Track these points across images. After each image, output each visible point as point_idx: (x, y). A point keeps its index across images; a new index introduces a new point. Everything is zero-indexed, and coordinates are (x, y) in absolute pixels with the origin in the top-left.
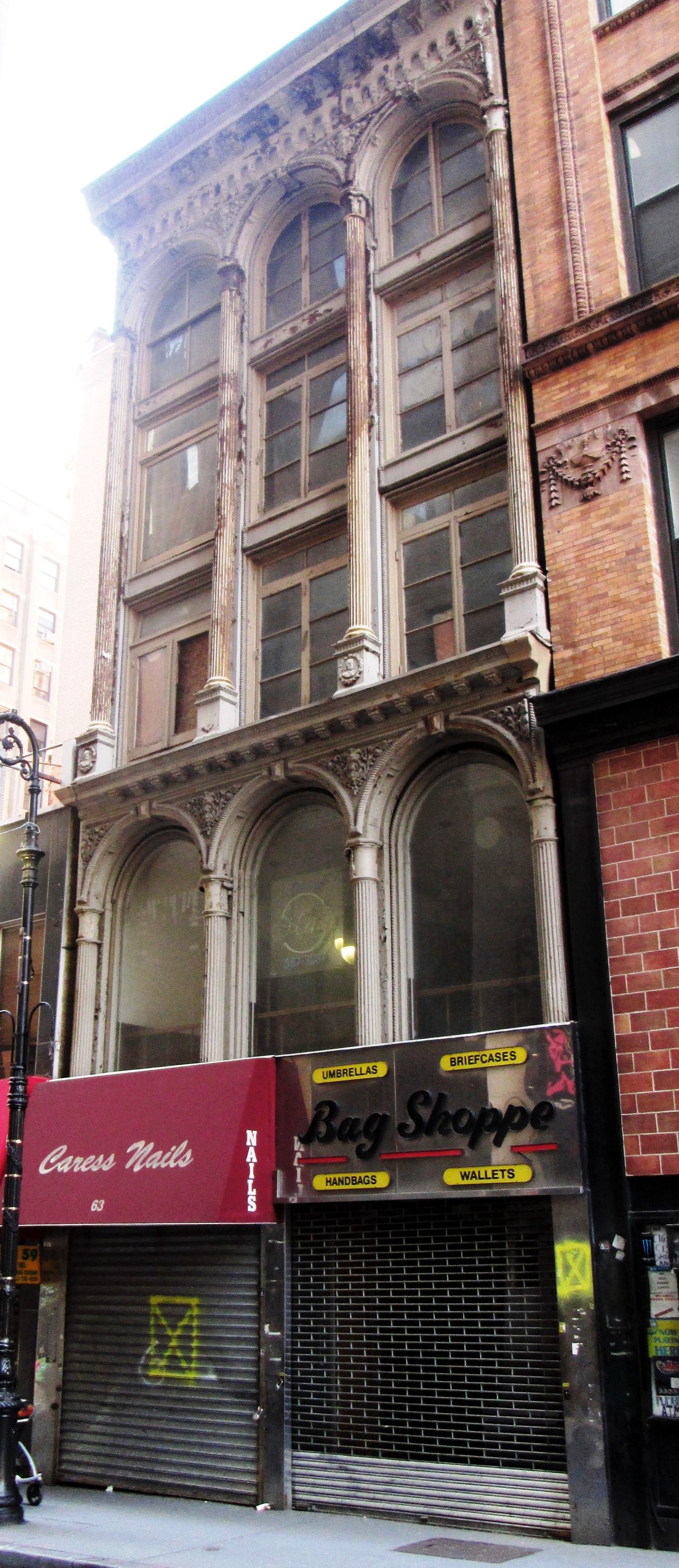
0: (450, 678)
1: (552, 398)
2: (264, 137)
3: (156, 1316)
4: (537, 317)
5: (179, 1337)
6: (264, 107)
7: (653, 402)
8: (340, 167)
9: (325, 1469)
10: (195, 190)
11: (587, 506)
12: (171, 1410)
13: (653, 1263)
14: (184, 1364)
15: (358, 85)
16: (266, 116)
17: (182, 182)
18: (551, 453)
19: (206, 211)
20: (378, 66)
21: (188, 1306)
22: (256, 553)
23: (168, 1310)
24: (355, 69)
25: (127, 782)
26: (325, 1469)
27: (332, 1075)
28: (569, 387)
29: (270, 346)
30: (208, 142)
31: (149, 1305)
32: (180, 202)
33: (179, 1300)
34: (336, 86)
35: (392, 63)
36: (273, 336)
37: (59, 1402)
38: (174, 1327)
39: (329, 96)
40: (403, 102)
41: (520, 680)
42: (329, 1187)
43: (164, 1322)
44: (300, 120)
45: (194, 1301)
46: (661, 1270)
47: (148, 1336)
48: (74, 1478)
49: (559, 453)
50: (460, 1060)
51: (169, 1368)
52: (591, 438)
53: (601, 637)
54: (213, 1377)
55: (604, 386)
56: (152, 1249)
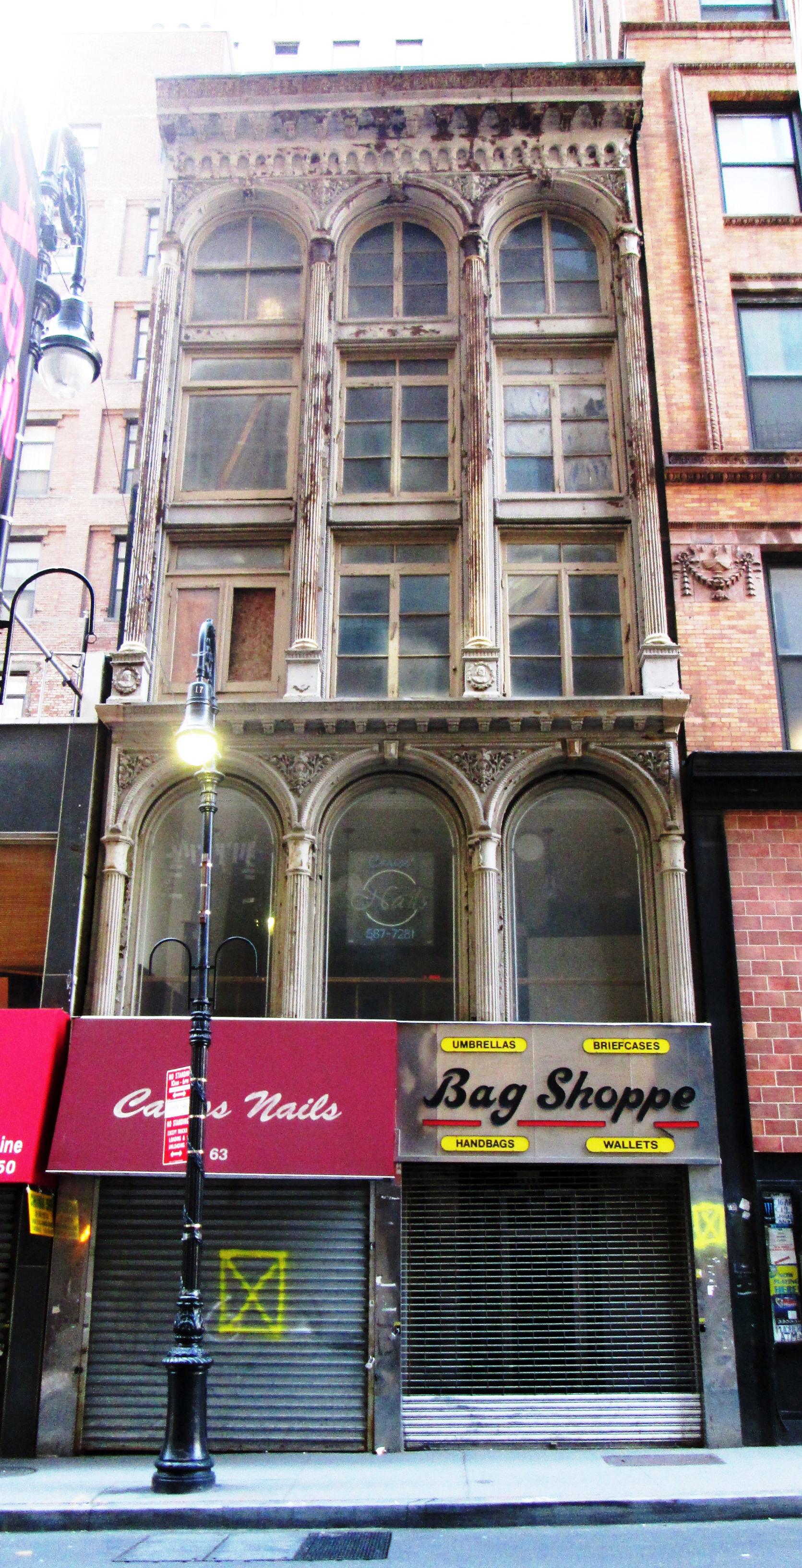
0: (602, 713)
1: (684, 503)
2: (382, 135)
3: (228, 1270)
4: (671, 431)
5: (260, 1292)
6: (399, 111)
7: (776, 541)
8: (468, 209)
9: (441, 1409)
10: (288, 145)
11: (716, 604)
12: (250, 1365)
13: (773, 1222)
14: (266, 1318)
15: (493, 143)
16: (395, 119)
17: (276, 130)
18: (683, 549)
19: (298, 173)
20: (517, 137)
21: (274, 1260)
22: (343, 530)
24: (494, 127)
26: (441, 1409)
27: (464, 1045)
28: (700, 500)
29: (362, 337)
30: (327, 111)
31: (219, 1259)
32: (270, 147)
33: (259, 1254)
34: (472, 133)
35: (532, 142)
36: (367, 328)
37: (84, 1365)
38: (253, 1281)
39: (462, 136)
40: (536, 181)
41: (661, 731)
42: (460, 1148)
43: (238, 1276)
44: (424, 141)
45: (282, 1255)
46: (780, 1226)
47: (218, 1291)
48: (104, 1446)
49: (692, 552)
50: (604, 1045)
51: (245, 1323)
52: (723, 551)
53: (729, 715)
54: (307, 1330)
55: (733, 513)
56: (223, 1202)
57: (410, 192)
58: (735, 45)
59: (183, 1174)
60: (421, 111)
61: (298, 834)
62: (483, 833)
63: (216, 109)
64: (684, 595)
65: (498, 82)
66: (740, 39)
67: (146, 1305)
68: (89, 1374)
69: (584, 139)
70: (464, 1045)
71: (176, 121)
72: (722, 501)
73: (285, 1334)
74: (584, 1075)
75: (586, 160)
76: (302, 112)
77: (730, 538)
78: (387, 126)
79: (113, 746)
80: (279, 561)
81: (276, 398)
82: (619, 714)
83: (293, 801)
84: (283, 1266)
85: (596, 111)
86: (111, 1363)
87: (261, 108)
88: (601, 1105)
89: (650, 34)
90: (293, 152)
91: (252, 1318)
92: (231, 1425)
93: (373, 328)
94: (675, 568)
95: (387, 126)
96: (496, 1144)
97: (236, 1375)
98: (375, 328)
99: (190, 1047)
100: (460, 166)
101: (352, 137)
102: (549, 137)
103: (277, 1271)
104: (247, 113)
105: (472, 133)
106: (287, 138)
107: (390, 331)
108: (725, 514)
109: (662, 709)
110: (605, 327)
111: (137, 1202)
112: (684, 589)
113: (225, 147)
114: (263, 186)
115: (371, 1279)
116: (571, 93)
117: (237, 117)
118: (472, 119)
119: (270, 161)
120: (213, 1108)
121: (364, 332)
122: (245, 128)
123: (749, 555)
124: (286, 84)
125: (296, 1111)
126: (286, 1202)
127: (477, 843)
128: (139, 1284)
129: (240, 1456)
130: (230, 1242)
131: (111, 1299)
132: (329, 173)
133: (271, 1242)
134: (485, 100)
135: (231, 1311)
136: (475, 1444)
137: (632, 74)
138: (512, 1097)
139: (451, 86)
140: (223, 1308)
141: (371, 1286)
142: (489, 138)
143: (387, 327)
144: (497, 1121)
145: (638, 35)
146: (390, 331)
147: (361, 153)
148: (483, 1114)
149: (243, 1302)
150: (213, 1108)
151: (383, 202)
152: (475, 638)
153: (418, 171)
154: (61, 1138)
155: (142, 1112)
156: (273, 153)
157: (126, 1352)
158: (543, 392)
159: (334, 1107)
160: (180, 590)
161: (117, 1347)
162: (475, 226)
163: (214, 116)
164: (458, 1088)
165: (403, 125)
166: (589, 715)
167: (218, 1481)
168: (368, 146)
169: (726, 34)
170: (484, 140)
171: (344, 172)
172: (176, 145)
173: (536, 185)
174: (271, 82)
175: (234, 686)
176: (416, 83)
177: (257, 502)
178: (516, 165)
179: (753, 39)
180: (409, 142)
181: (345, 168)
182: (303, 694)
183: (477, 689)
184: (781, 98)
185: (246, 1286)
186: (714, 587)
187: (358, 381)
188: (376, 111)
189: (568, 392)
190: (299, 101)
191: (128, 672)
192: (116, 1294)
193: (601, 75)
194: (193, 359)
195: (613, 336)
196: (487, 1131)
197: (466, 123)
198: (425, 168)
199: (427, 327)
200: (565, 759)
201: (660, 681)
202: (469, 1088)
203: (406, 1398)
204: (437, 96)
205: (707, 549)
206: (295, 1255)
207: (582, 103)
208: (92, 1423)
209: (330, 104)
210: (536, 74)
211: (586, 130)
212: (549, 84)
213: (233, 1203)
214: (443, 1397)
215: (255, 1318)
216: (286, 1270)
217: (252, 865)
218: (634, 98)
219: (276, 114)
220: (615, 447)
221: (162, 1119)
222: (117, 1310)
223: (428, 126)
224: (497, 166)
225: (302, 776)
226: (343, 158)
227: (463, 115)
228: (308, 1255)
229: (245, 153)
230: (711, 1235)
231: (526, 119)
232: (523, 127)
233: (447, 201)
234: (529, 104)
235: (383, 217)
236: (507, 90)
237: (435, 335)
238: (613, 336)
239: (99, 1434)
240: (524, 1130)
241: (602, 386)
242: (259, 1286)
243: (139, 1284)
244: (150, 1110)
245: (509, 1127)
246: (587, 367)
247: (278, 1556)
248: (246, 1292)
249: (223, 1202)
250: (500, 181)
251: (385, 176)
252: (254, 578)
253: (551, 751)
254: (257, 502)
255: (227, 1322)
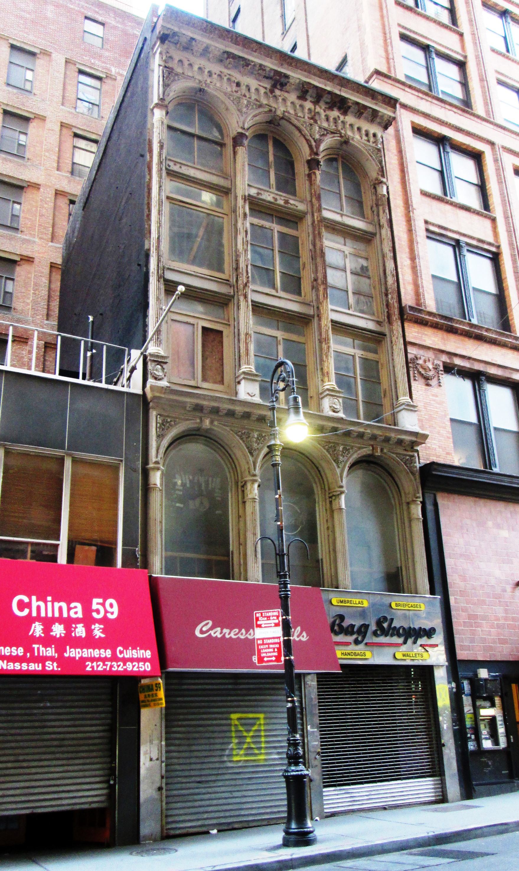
0: (393, 435)
1: (414, 333)
2: (274, 86)
3: (236, 725)
4: (405, 293)
5: (252, 737)
6: (287, 77)
7: (448, 361)
8: (313, 144)
9: (337, 795)
10: (226, 71)
11: (427, 387)
12: (250, 778)
13: (464, 693)
14: (256, 751)
15: (325, 111)
16: (283, 80)
17: (221, 61)
18: (413, 356)
19: (229, 90)
20: (335, 113)
21: (258, 719)
22: (257, 306)
23: (243, 721)
24: (327, 103)
25: (205, 403)
26: (337, 795)
27: (342, 602)
28: (418, 333)
29: (260, 197)
30: (253, 62)
31: (231, 719)
32: (216, 68)
33: (251, 715)
34: (316, 102)
35: (342, 118)
36: (262, 192)
37: (164, 785)
38: (248, 731)
39: (311, 101)
40: (343, 140)
41: (412, 448)
42: (343, 657)
43: (241, 728)
44: (292, 97)
45: (262, 716)
46: (466, 695)
47: (231, 737)
48: (178, 832)
49: (417, 358)
50: (399, 605)
51: (246, 755)
52: (429, 361)
53: (435, 444)
54: (276, 756)
55: (431, 342)
56: (230, 687)
57: (283, 122)
58: (420, 100)
59: (283, 671)
60: (298, 81)
61: (254, 478)
62: (341, 489)
63: (195, 36)
64: (415, 380)
65: (336, 81)
66: (422, 98)
67: (194, 748)
68: (166, 790)
69: (365, 126)
70: (342, 602)
71: (171, 33)
72: (426, 335)
73: (266, 760)
74: (392, 620)
75: (372, 139)
76: (240, 57)
77: (430, 355)
78: (279, 82)
79: (151, 410)
80: (222, 316)
81: (216, 218)
82: (399, 437)
83: (251, 459)
84: (262, 722)
85: (375, 114)
86: (178, 783)
87: (220, 46)
88: (399, 636)
89: (386, 80)
90: (228, 76)
91: (249, 751)
92: (243, 812)
93: (266, 193)
94: (410, 365)
95: (279, 82)
96: (358, 655)
97: (243, 785)
98: (267, 194)
99: (279, 600)
100: (308, 118)
101: (260, 81)
102: (350, 119)
103: (260, 724)
104: (211, 45)
105: (316, 102)
106: (226, 67)
107: (274, 198)
108: (428, 342)
109: (417, 438)
110: (369, 228)
111: (185, 687)
112: (415, 376)
113: (193, 59)
114: (210, 90)
115: (305, 727)
116: (366, 101)
117: (205, 45)
118: (319, 95)
119: (215, 76)
120: (246, 634)
121: (261, 194)
122: (206, 52)
123: (439, 365)
124: (234, 37)
125: (229, 634)
126: (261, 686)
127: (338, 495)
128: (190, 736)
129: (250, 829)
130: (235, 709)
131: (175, 745)
132: (245, 96)
133: (255, 708)
134: (328, 88)
135: (239, 749)
136: (353, 811)
137: (393, 102)
138: (363, 630)
139: (315, 75)
140: (235, 747)
141: (305, 731)
142: (323, 108)
143: (272, 195)
144: (357, 642)
145: (381, 78)
146: (274, 198)
147: (262, 91)
148: (350, 639)
149: (244, 743)
150: (246, 634)
151: (267, 122)
152: (330, 383)
153: (289, 113)
154: (172, 650)
155: (210, 634)
156: (218, 73)
157: (186, 777)
158: (342, 254)
159: (304, 634)
160: (172, 320)
161: (180, 773)
162: (317, 154)
163: (193, 39)
164: (340, 626)
165: (286, 84)
166: (387, 434)
167: (319, 838)
168: (266, 88)
169: (416, 93)
170: (321, 108)
171: (253, 98)
172: (165, 46)
173: (341, 141)
174: (226, 33)
175: (205, 385)
176: (298, 65)
177: (209, 277)
178: (334, 127)
179: (427, 101)
180: (286, 95)
181: (254, 97)
182: (253, 398)
183: (334, 411)
184: (436, 135)
185: (245, 734)
186: (427, 379)
187: (256, 221)
188: (276, 72)
189: (352, 257)
190: (239, 50)
191: (159, 367)
192: (177, 742)
193: (380, 97)
194: (171, 180)
195: (374, 235)
196: (352, 648)
197: (315, 96)
198: (292, 112)
199: (291, 202)
200: (371, 455)
201: (408, 422)
202: (345, 624)
203: (324, 790)
204: (307, 77)
205: (423, 358)
206: (268, 715)
207: (370, 108)
208: (170, 819)
209: (256, 59)
210: (353, 85)
211: (366, 122)
212: (358, 92)
213: (236, 687)
214: (338, 788)
215: (250, 752)
216: (264, 724)
217: (181, 488)
218: (392, 115)
219: (225, 52)
220: (376, 293)
221: (254, 639)
222: (179, 752)
223: (296, 89)
224: (325, 125)
225: (255, 445)
226: (253, 90)
227: (315, 91)
228: (273, 715)
229: (202, 66)
230: (444, 700)
231: (341, 104)
232: (339, 109)
233: (302, 134)
234: (347, 99)
235: (264, 130)
236: (339, 87)
237: (295, 208)
238: (374, 235)
239: (173, 826)
240: (368, 648)
241: (367, 259)
242: (251, 734)
243: (190, 736)
244: (215, 633)
245: (361, 646)
246: (361, 246)
247: (418, 867)
248: (246, 737)
249: (230, 687)
250: (327, 133)
251: (274, 110)
252: (216, 324)
253: (366, 451)
254: (209, 277)
255: (237, 755)
